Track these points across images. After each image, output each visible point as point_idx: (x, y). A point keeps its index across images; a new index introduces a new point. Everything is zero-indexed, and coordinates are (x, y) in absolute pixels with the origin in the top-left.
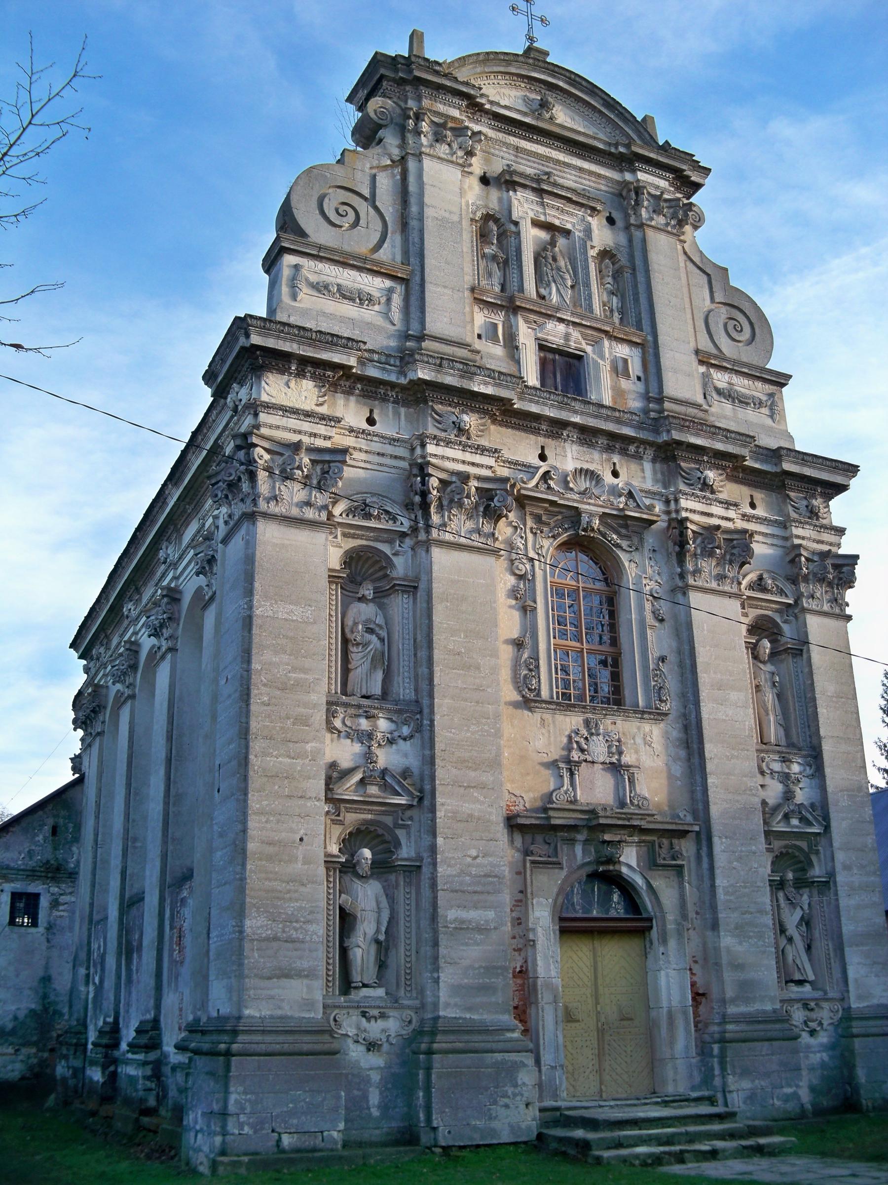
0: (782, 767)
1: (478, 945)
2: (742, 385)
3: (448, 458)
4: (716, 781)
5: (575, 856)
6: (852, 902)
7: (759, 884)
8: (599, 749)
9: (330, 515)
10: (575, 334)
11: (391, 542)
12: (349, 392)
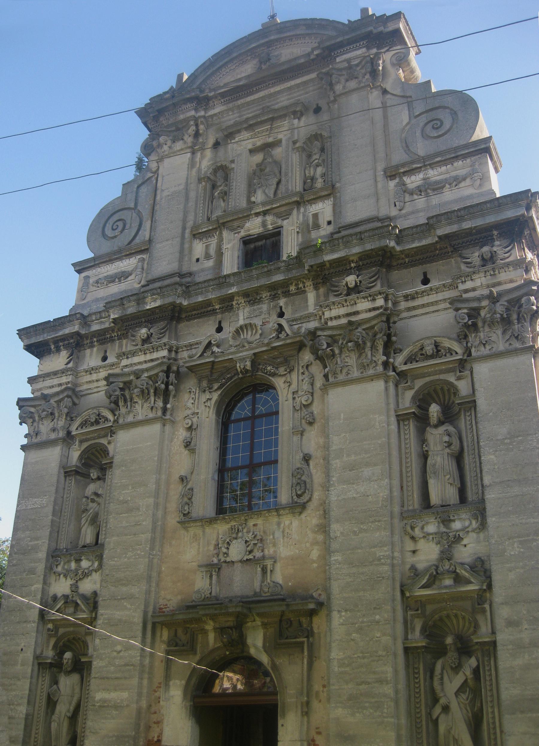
0: (438, 527)
1: (114, 719)
2: (435, 174)
3: (135, 364)
4: (340, 558)
5: (208, 643)
6: (519, 662)
7: (380, 653)
8: (236, 551)
9: (69, 433)
10: (269, 219)
11: (106, 436)
12: (92, 346)
